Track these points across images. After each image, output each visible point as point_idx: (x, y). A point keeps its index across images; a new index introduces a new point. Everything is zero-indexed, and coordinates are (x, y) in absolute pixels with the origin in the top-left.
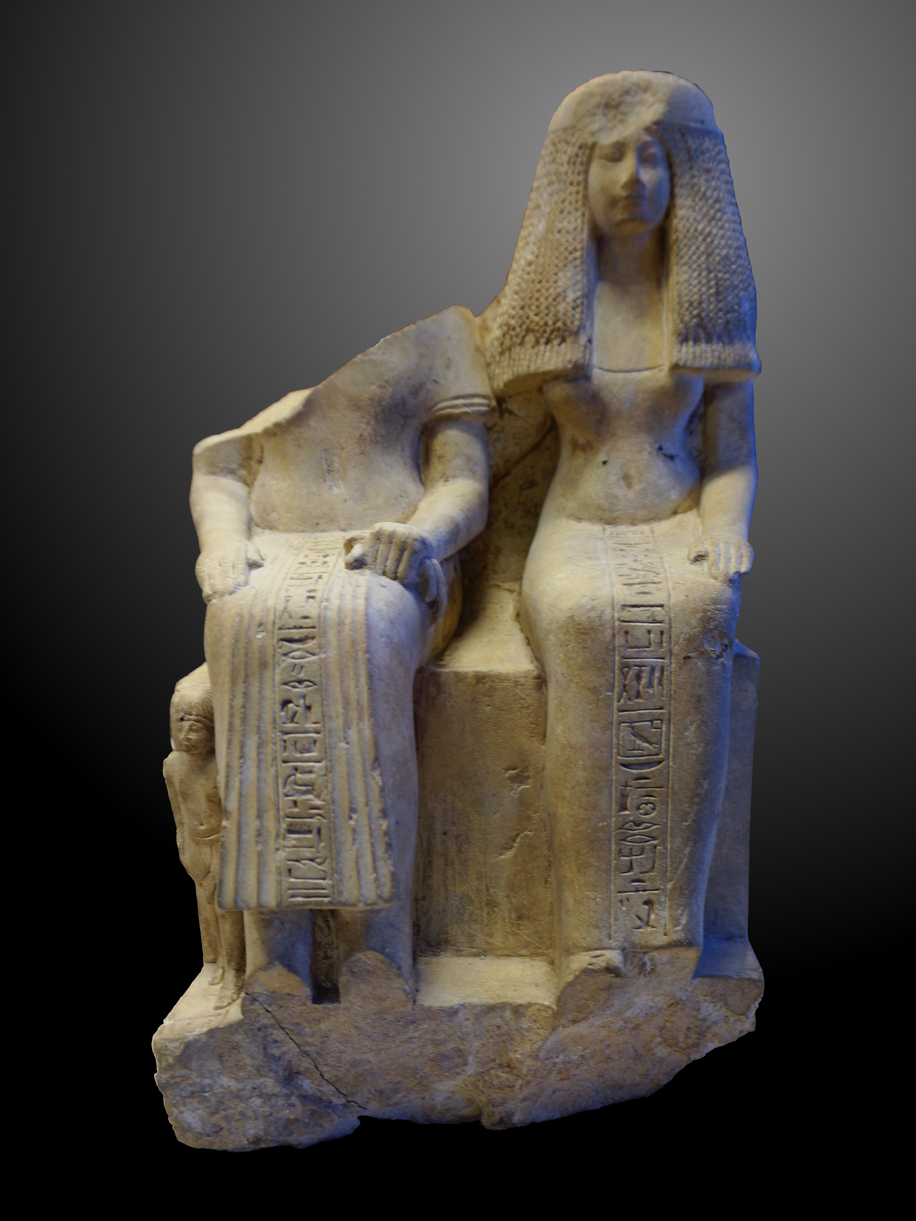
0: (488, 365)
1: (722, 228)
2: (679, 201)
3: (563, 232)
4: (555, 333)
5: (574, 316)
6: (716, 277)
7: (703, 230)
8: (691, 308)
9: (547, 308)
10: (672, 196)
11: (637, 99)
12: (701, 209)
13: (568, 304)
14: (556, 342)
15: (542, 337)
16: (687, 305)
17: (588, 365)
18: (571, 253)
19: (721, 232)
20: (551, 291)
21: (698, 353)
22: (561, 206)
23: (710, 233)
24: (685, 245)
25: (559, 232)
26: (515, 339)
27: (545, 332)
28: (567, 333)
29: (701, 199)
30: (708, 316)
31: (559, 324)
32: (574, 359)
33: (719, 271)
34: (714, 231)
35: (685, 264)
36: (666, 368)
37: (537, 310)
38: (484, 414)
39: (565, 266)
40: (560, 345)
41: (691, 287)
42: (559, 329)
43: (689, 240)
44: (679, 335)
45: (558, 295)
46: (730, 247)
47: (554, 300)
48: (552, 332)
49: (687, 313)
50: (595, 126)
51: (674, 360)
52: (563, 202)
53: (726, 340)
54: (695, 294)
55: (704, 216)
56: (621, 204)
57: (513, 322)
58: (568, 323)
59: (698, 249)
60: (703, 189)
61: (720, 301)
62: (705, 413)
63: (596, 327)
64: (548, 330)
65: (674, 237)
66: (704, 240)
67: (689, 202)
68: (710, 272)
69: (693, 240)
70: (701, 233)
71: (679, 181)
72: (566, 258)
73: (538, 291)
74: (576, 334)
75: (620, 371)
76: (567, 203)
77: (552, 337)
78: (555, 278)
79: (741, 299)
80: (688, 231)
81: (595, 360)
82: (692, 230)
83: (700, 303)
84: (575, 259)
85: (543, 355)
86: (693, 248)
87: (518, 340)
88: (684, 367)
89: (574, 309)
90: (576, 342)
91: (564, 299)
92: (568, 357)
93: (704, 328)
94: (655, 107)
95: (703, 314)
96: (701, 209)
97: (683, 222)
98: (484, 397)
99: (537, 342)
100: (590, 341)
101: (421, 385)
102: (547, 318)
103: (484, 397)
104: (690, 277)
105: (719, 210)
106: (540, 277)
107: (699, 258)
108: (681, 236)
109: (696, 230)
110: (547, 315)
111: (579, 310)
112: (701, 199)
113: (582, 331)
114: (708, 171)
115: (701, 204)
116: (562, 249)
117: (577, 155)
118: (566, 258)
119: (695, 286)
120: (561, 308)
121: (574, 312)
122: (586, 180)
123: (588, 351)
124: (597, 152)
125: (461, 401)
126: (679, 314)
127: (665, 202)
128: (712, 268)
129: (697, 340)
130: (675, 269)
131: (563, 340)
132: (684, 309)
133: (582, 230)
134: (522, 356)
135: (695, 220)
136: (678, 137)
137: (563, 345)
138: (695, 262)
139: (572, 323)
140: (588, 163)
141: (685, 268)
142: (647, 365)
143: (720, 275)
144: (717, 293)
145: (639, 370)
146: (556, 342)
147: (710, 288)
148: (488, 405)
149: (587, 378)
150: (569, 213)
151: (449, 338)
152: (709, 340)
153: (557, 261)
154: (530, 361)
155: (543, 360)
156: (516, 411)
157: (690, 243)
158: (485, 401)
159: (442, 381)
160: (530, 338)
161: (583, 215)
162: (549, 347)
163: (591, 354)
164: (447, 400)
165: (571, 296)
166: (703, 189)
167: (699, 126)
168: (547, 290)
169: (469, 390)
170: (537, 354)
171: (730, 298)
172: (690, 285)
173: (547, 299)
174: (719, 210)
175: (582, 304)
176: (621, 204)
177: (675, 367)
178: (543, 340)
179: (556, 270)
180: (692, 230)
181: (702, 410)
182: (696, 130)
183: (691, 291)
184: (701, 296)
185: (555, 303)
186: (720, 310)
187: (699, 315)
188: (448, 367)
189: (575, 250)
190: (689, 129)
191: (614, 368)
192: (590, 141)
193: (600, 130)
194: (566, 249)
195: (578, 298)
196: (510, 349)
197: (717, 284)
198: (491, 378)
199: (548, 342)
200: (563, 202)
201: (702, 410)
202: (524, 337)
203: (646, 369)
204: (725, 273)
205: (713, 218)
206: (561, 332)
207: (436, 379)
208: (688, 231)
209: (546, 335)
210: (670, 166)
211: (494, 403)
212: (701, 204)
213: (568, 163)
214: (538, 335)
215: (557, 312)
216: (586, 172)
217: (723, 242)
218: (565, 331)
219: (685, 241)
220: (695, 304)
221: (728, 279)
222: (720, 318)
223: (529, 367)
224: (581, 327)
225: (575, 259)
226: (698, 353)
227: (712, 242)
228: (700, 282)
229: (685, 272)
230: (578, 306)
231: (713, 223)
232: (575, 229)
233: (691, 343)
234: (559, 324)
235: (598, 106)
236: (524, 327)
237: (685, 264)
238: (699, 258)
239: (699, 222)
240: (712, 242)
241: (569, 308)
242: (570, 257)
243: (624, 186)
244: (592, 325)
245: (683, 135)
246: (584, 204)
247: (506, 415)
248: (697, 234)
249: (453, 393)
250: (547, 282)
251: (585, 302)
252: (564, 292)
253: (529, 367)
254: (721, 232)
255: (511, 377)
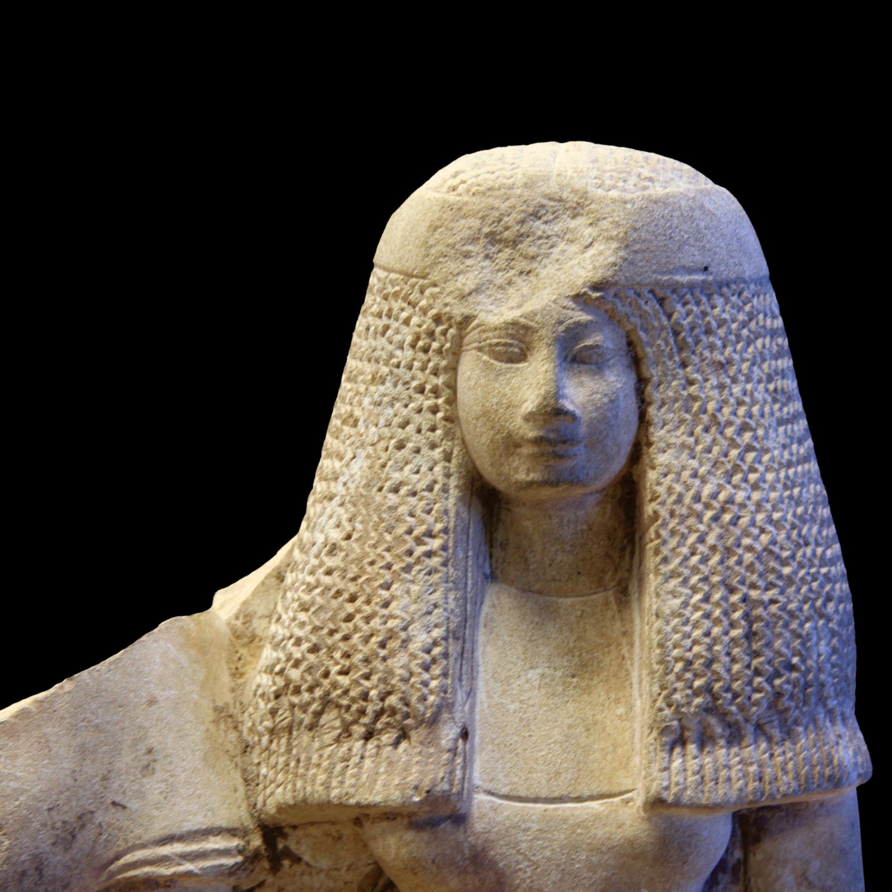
0: (247, 748)
1: (755, 487)
2: (657, 434)
3: (403, 490)
4: (384, 719)
5: (425, 684)
6: (745, 599)
7: (714, 496)
8: (689, 675)
9: (367, 660)
10: (643, 420)
11: (557, 228)
12: (709, 450)
13: (413, 656)
14: (387, 738)
15: (355, 722)
16: (679, 666)
17: (460, 793)
18: (419, 541)
19: (756, 496)
20: (376, 622)
21: (708, 770)
22: (400, 434)
23: (730, 501)
24: (673, 533)
25: (396, 490)
26: (299, 714)
27: (362, 712)
28: (409, 721)
29: (706, 430)
30: (728, 689)
31: (392, 700)
32: (426, 784)
33: (753, 586)
34: (740, 496)
35: (674, 574)
36: (639, 799)
37: (347, 663)
38: (232, 871)
39: (407, 569)
40: (396, 744)
41: (688, 629)
42: (393, 711)
43: (683, 518)
44: (664, 731)
45: (391, 635)
46: (777, 524)
47: (383, 645)
48: (379, 714)
49: (679, 685)
50: (467, 282)
51: (654, 788)
52: (404, 425)
53: (776, 734)
54: (695, 642)
55: (715, 464)
56: (526, 450)
57: (295, 674)
58: (414, 700)
59: (701, 540)
60: (711, 406)
61: (756, 654)
62: (745, 861)
63: (481, 695)
64: (370, 709)
65: (649, 509)
66: (716, 519)
67: (680, 437)
68: (732, 590)
69: (692, 521)
70: (707, 506)
71: (655, 394)
72: (410, 553)
73: (349, 618)
74: (434, 722)
75: (536, 800)
76: (410, 428)
77: (379, 726)
78: (385, 594)
79: (805, 639)
80: (679, 500)
81: (477, 776)
82: (687, 500)
83: (709, 663)
84: (429, 554)
85: (359, 765)
86: (692, 538)
87: (307, 719)
88: (677, 803)
89: (426, 668)
90: (432, 741)
91: (405, 642)
92: (413, 778)
93: (723, 716)
94: (598, 247)
95: (717, 686)
96: (709, 450)
97: (667, 481)
98: (232, 832)
99: (346, 731)
100: (465, 734)
101: (83, 819)
102: (366, 683)
103: (232, 832)
104: (685, 604)
105: (749, 448)
106: (352, 588)
107: (705, 560)
108: (664, 513)
109: (697, 498)
110: (367, 677)
111: (436, 670)
112: (706, 430)
113: (445, 716)
114: (722, 366)
115: (708, 438)
116: (401, 530)
117: (431, 334)
118: (410, 553)
119: (695, 626)
120: (398, 663)
121: (426, 676)
122: (452, 386)
123: (459, 760)
124: (472, 336)
125: (178, 848)
126: (663, 688)
127: (626, 438)
128: (734, 582)
129: (705, 741)
130: (653, 582)
131: (404, 735)
132: (672, 677)
133: (445, 490)
134: (315, 758)
135: (695, 475)
136: (653, 306)
137: (404, 745)
138: (695, 570)
139: (423, 699)
140: (456, 352)
141: (674, 583)
142: (595, 790)
143: (754, 594)
144: (750, 636)
145: (579, 799)
146: (387, 738)
147: (733, 625)
148: (240, 852)
149: (460, 819)
150: (418, 451)
151: (152, 702)
152: (735, 737)
153: (388, 557)
154: (329, 771)
155: (357, 776)
156: (306, 858)
157: (683, 529)
158: (234, 843)
159: (133, 805)
160: (330, 718)
161: (448, 457)
162: (371, 745)
163: (467, 765)
164: (143, 846)
165: (420, 638)
166: (711, 406)
167: (699, 277)
168: (368, 619)
169: (199, 821)
170: (346, 759)
171: (778, 644)
172: (686, 623)
173: (366, 640)
174: (749, 448)
175: (446, 655)
176: (526, 450)
177: (656, 804)
178: (358, 730)
179: (388, 576)
180: (687, 500)
181: (738, 854)
182: (691, 287)
183: (687, 636)
184: (710, 648)
185: (383, 653)
186: (757, 672)
187: (707, 689)
188: (147, 769)
189: (430, 534)
190: (675, 288)
191: (523, 793)
192: (458, 311)
193: (477, 290)
194: (410, 532)
195: (435, 643)
196: (290, 729)
197: (746, 616)
198: (250, 781)
199: (368, 736)
200: (404, 425)
201: (738, 854)
202: (318, 714)
203: (592, 798)
204: (767, 589)
205: (736, 468)
206: (398, 717)
207: (118, 799)
208: (679, 500)
209: (365, 720)
210: (636, 362)
211: (257, 842)
212: (708, 438)
213: (413, 346)
214: (348, 717)
215: (390, 672)
216: (453, 369)
217: (760, 517)
218: (407, 716)
219: (673, 523)
220: (698, 665)
221: (773, 601)
222: (758, 690)
223: (327, 786)
224: (444, 706)
225: (429, 554)
226: (708, 770)
227: (735, 522)
228: (707, 616)
229: (674, 594)
230: (434, 661)
231: (737, 478)
232: (430, 489)
233: (692, 748)
234: (392, 700)
235: (474, 240)
236: (318, 693)
237: (674, 574)
238: (705, 560)
239: (704, 481)
240: (735, 522)
241: (415, 667)
242: (419, 550)
243: (530, 417)
244: (471, 693)
245: (661, 301)
246: (448, 435)
247: (286, 863)
248: (699, 507)
249: (158, 830)
250: (368, 602)
251: (454, 648)
252: (405, 629)
253: (327, 786)
254: (756, 496)
255: (289, 798)
